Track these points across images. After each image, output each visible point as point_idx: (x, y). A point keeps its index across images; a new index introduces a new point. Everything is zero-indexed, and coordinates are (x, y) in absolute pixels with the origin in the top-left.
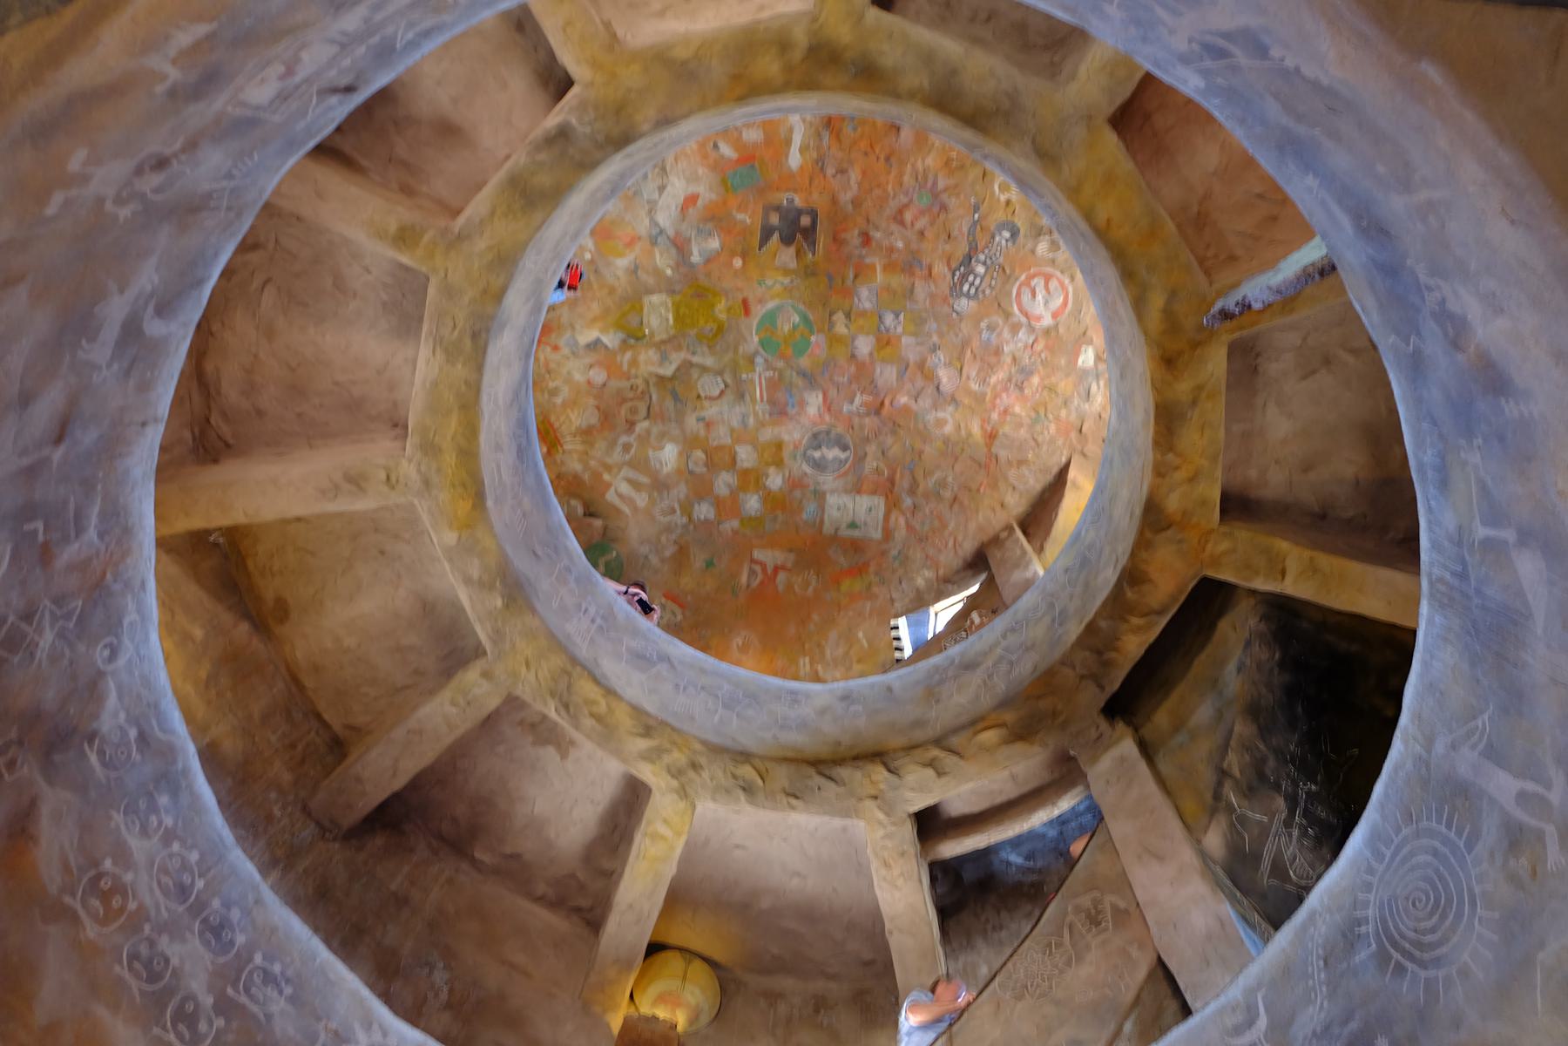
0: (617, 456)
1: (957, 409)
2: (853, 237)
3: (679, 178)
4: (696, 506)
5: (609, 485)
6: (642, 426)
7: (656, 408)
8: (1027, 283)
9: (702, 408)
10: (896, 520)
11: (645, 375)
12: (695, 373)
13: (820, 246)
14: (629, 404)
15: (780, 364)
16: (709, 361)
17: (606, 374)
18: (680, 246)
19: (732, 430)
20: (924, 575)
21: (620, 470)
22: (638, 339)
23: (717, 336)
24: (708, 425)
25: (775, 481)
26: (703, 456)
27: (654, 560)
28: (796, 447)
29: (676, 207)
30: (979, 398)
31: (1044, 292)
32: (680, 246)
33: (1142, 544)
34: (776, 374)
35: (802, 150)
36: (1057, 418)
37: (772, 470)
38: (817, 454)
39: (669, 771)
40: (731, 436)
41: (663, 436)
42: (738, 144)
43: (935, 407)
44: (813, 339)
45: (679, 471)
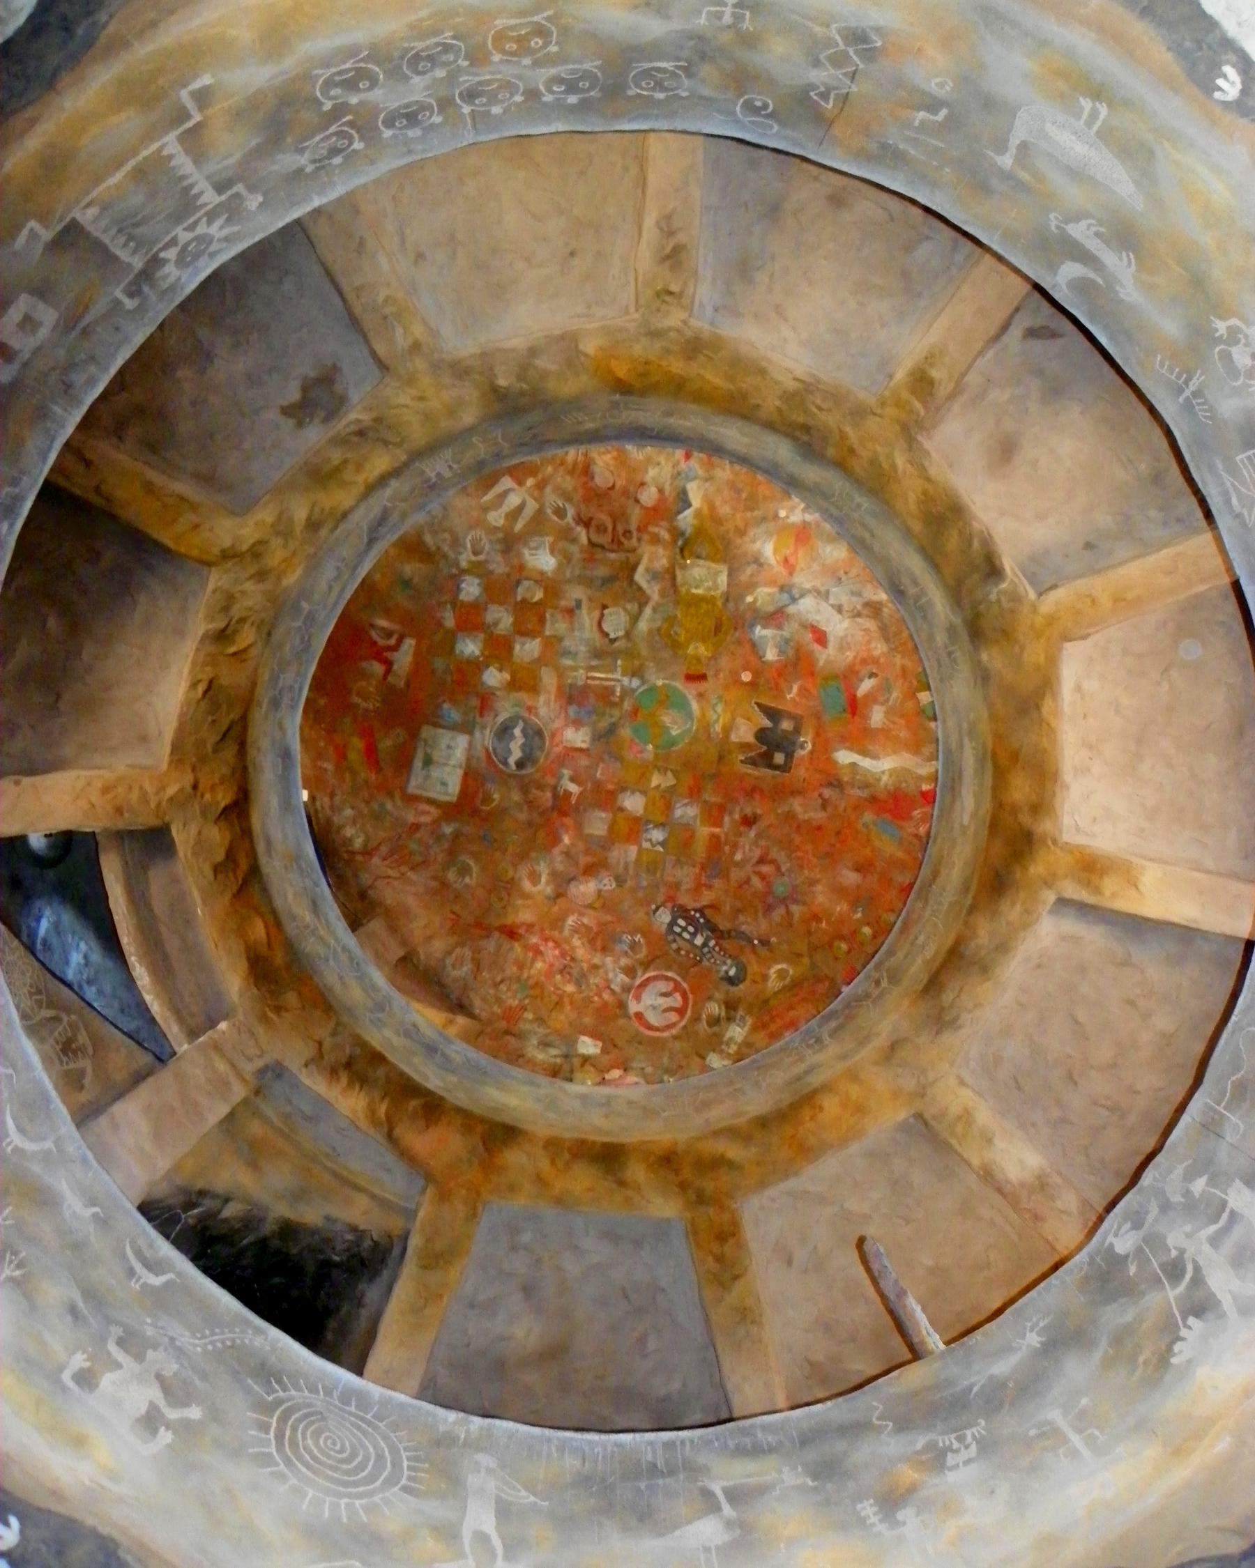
0: (552, 498)
1: (548, 898)
2: (756, 807)
3: (846, 629)
4: (477, 581)
5: (521, 483)
6: (582, 534)
7: (599, 555)
8: (677, 987)
9: (590, 610)
10: (428, 813)
11: (640, 551)
12: (633, 607)
13: (749, 770)
15: (627, 705)
16: (643, 626)
17: (649, 505)
18: (776, 617)
19: (560, 639)
20: (359, 837)
21: (536, 500)
23: (667, 640)
24: (571, 612)
25: (493, 677)
26: (536, 599)
28: (529, 709)
29: (818, 621)
30: (558, 922)
31: (665, 1006)
32: (776, 617)
33: (469, 1120)
34: (617, 699)
35: (854, 765)
36: (524, 1009)
37: (507, 676)
38: (517, 732)
39: (260, 542)
40: (555, 637)
41: (567, 558)
42: (871, 698)
43: (554, 875)
44: (650, 747)
45: (522, 568)
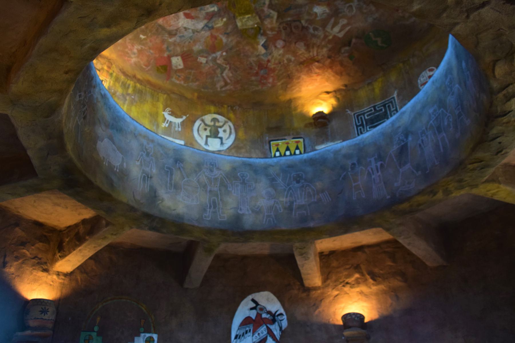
3: (179, 23)
11: (278, 24)
14: (293, 30)
21: (327, 31)
22: (260, 29)
27: (376, 15)
29: (192, 21)
41: (309, 14)
